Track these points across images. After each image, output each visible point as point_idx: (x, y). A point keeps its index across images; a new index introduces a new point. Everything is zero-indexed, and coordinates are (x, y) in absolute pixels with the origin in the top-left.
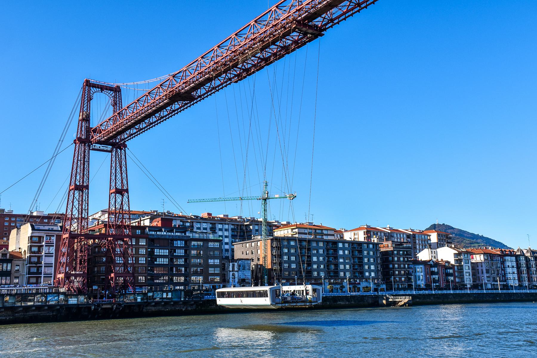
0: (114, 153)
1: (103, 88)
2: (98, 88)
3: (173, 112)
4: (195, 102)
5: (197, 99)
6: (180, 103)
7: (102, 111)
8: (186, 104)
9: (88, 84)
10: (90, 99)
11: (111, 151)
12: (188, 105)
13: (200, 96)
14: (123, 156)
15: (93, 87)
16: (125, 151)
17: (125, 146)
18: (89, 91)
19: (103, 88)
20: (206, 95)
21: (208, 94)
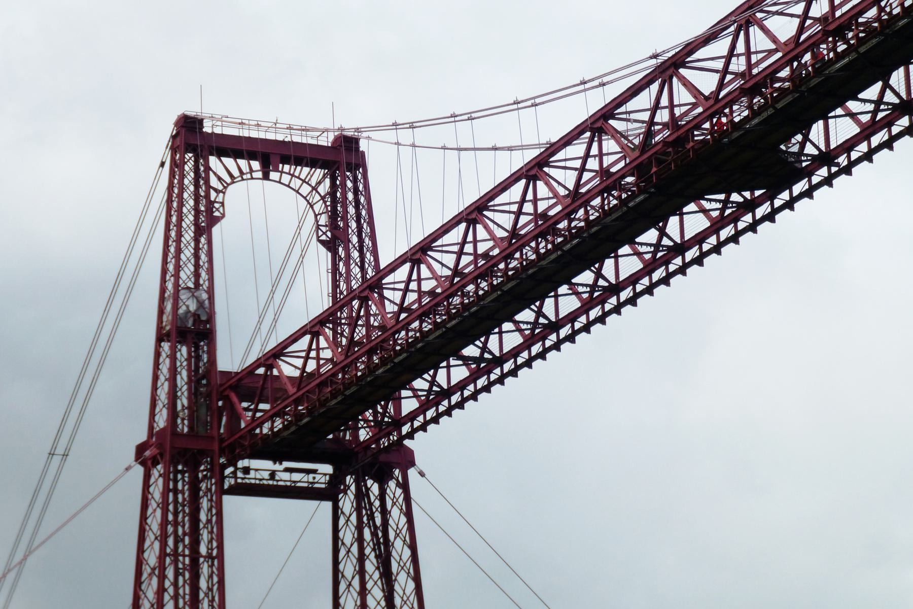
0: (347, 503)
1: (271, 155)
2: (251, 156)
3: (669, 261)
4: (798, 188)
5: (808, 173)
6: (712, 203)
7: (273, 281)
8: (749, 206)
9: (192, 139)
10: (208, 219)
11: (331, 493)
12: (760, 212)
13: (826, 158)
14: (396, 517)
15: (221, 153)
16: (405, 486)
17: (408, 460)
18: (201, 177)
19: (271, 155)
20: (863, 147)
21: (876, 140)
